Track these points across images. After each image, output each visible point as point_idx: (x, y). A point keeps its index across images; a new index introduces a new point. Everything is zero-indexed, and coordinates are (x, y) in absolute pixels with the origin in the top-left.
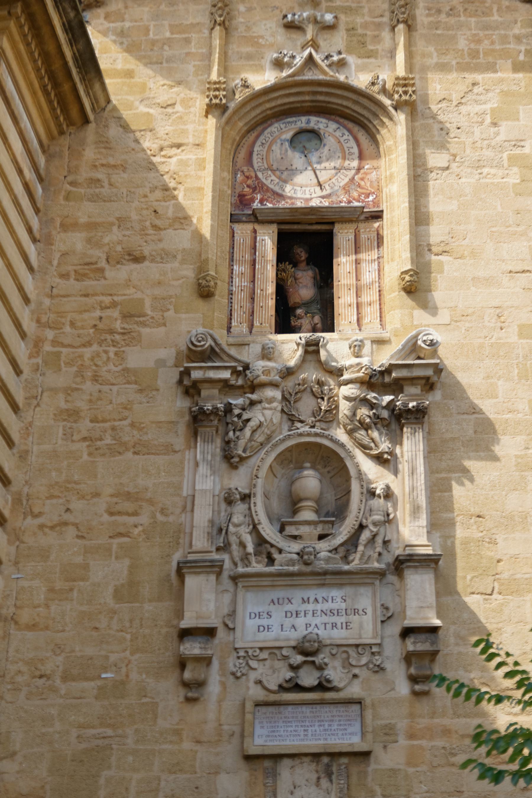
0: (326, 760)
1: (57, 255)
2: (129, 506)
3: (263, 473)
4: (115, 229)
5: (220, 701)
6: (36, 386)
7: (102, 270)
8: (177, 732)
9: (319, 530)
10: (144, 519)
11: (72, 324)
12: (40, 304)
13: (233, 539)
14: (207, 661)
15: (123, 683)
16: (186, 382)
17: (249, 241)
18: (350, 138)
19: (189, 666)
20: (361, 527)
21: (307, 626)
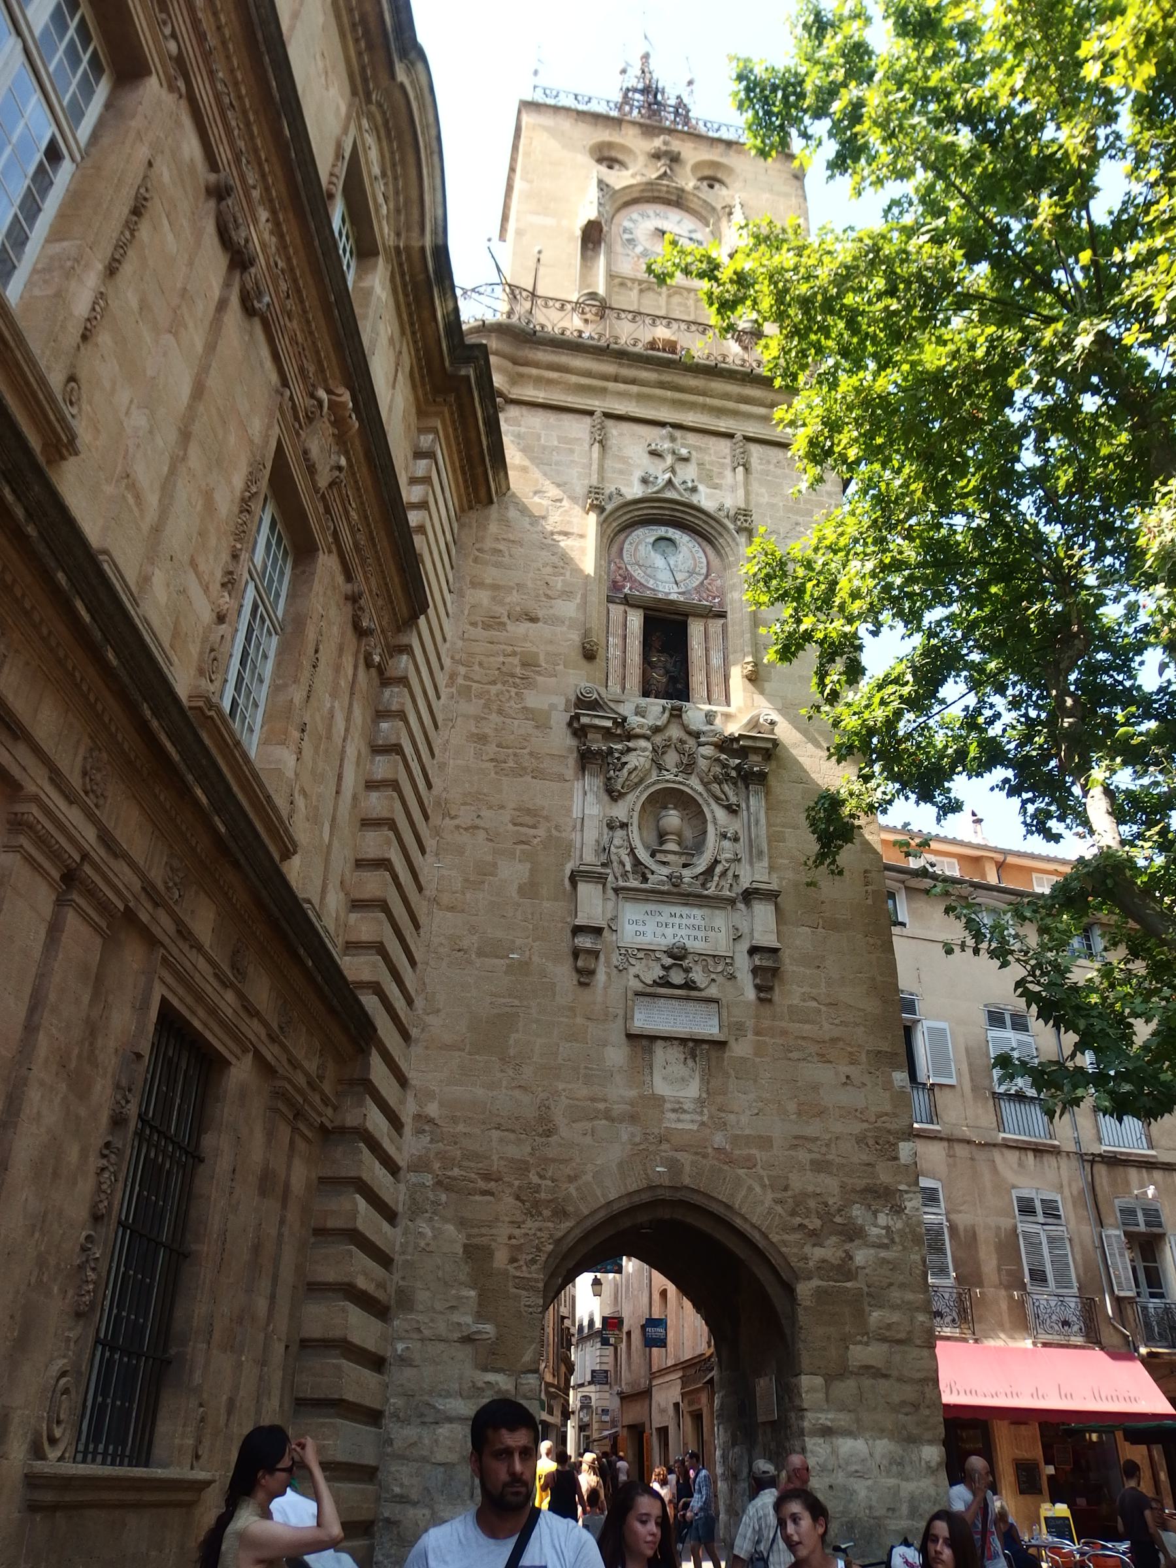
0: (691, 1044)
2: (528, 820)
3: (638, 808)
5: (605, 988)
7: (504, 624)
8: (572, 1009)
9: (683, 860)
10: (541, 832)
11: (480, 664)
13: (613, 858)
14: (596, 954)
15: (527, 963)
16: (575, 725)
17: (621, 619)
19: (582, 957)
21: (675, 936)
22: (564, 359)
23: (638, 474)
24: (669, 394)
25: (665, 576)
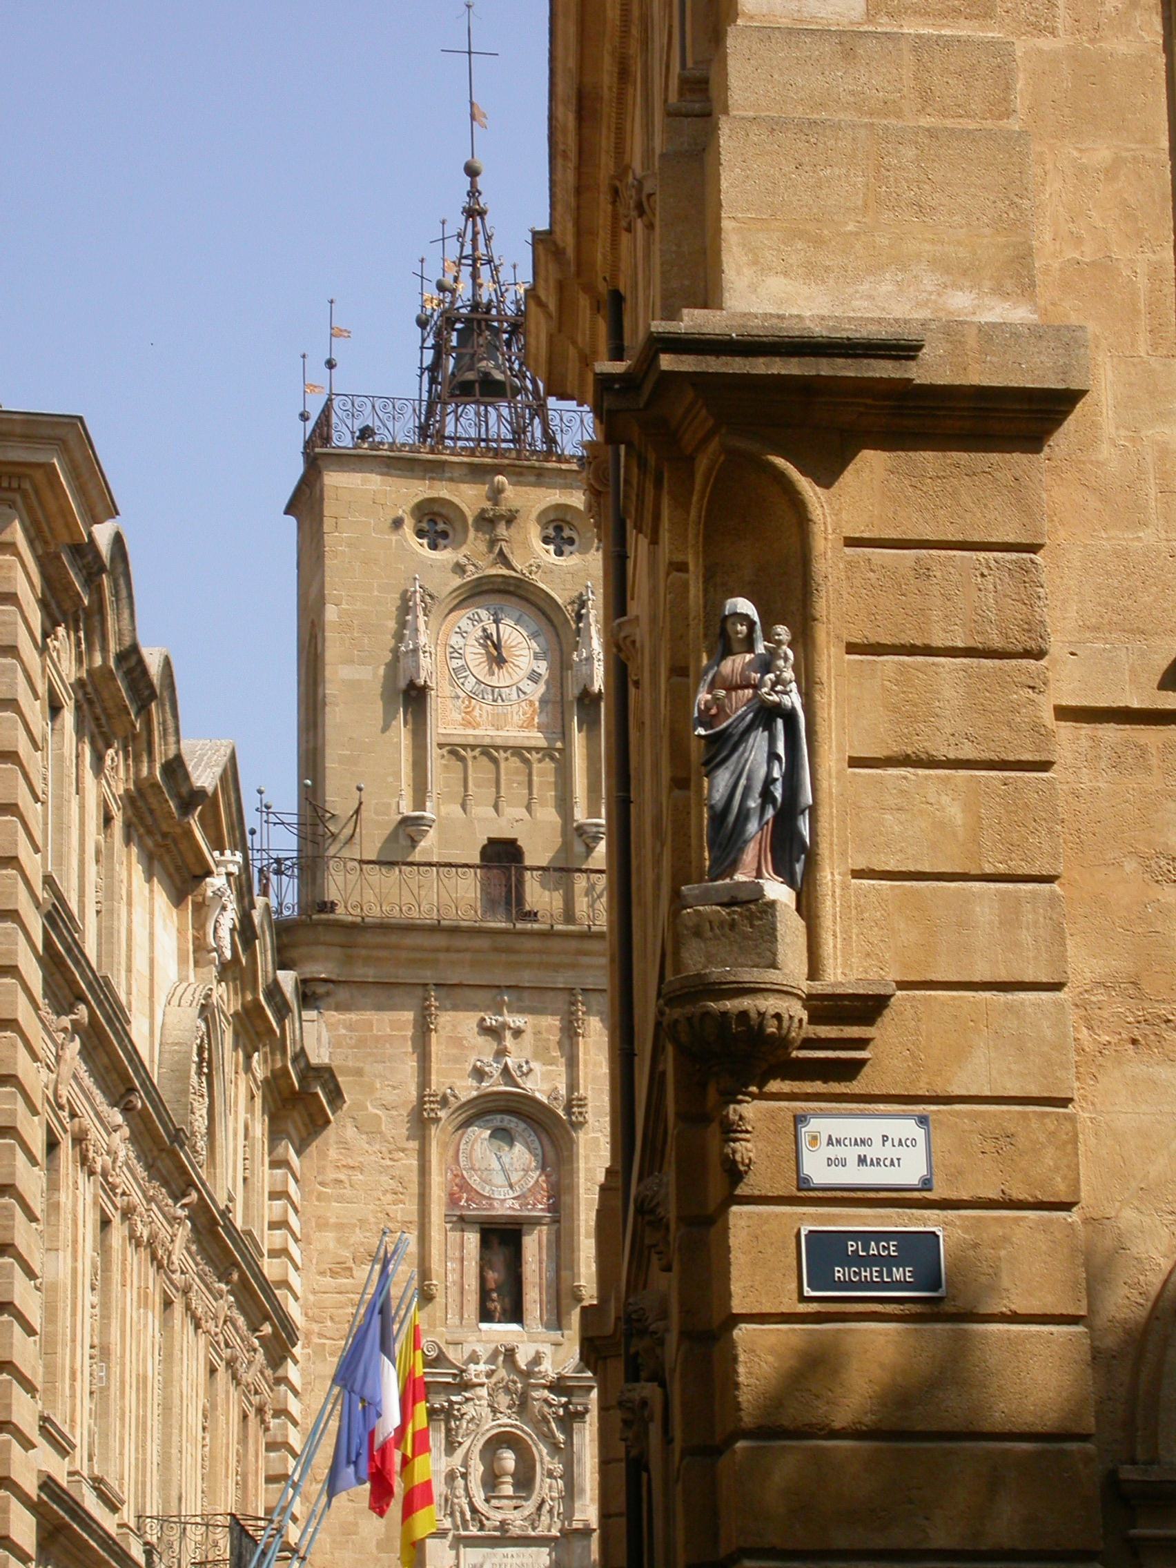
1: (315, 1254)
4: (357, 1230)
6: (310, 1374)
7: (350, 1269)
11: (332, 1318)
12: (306, 1299)
18: (537, 1142)
20: (543, 1501)
22: (394, 939)
23: (472, 1060)
24: (504, 957)
25: (499, 1179)
